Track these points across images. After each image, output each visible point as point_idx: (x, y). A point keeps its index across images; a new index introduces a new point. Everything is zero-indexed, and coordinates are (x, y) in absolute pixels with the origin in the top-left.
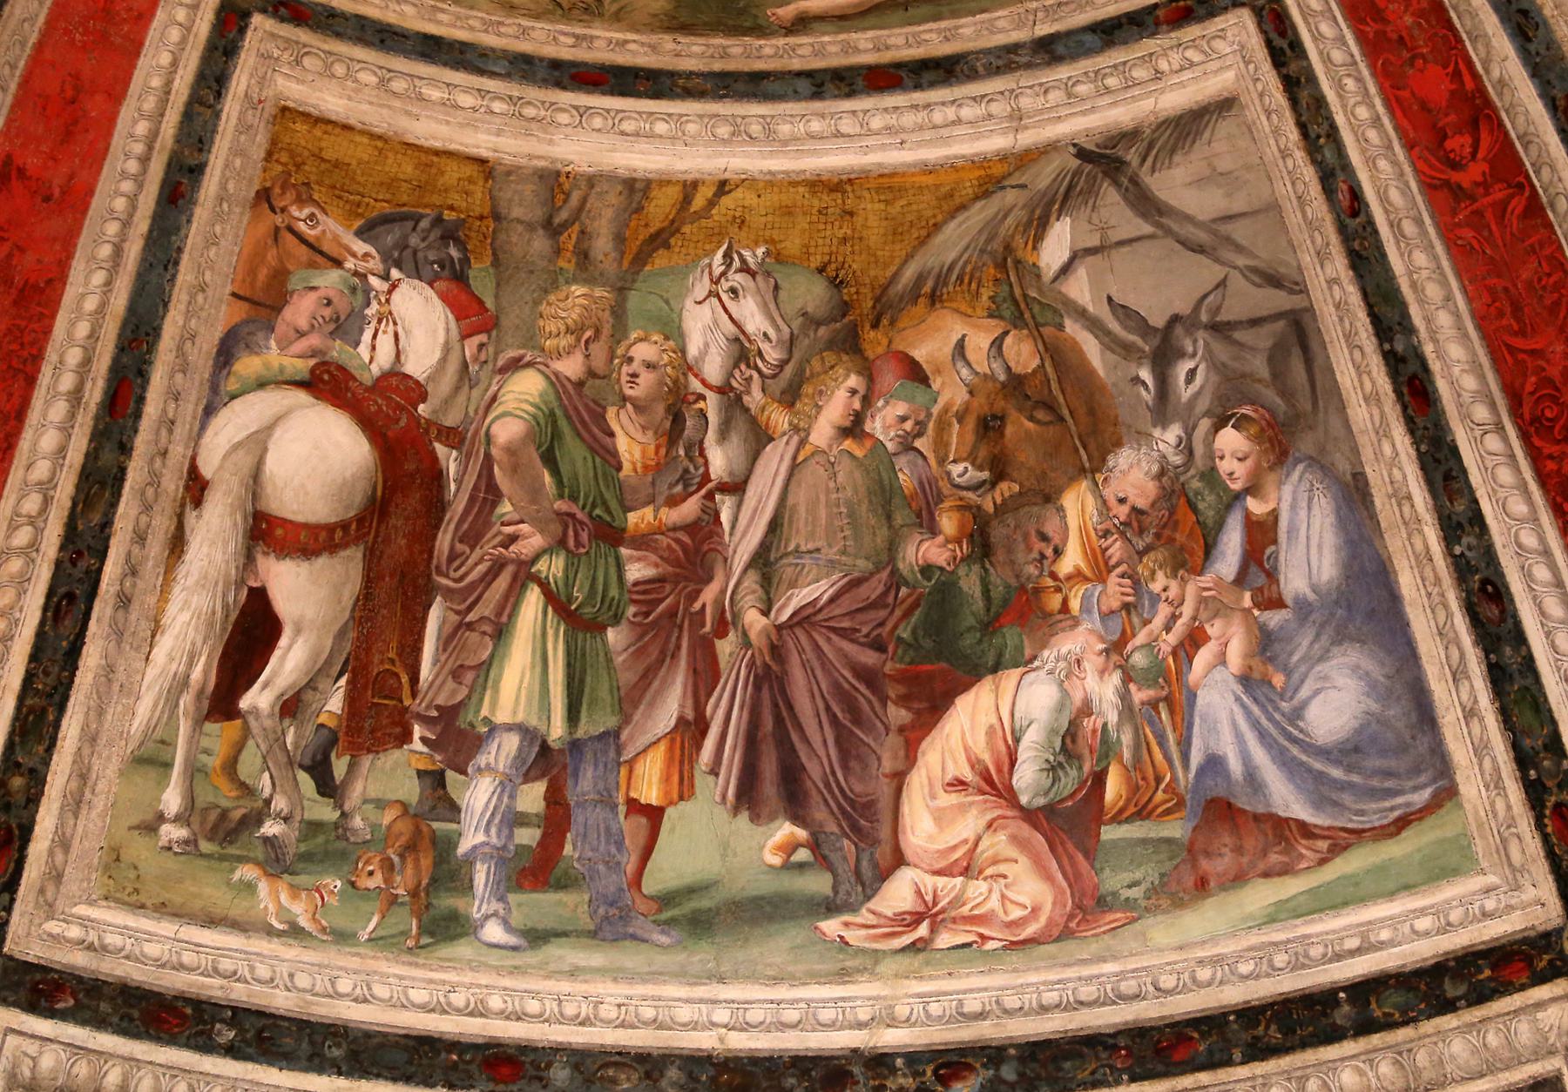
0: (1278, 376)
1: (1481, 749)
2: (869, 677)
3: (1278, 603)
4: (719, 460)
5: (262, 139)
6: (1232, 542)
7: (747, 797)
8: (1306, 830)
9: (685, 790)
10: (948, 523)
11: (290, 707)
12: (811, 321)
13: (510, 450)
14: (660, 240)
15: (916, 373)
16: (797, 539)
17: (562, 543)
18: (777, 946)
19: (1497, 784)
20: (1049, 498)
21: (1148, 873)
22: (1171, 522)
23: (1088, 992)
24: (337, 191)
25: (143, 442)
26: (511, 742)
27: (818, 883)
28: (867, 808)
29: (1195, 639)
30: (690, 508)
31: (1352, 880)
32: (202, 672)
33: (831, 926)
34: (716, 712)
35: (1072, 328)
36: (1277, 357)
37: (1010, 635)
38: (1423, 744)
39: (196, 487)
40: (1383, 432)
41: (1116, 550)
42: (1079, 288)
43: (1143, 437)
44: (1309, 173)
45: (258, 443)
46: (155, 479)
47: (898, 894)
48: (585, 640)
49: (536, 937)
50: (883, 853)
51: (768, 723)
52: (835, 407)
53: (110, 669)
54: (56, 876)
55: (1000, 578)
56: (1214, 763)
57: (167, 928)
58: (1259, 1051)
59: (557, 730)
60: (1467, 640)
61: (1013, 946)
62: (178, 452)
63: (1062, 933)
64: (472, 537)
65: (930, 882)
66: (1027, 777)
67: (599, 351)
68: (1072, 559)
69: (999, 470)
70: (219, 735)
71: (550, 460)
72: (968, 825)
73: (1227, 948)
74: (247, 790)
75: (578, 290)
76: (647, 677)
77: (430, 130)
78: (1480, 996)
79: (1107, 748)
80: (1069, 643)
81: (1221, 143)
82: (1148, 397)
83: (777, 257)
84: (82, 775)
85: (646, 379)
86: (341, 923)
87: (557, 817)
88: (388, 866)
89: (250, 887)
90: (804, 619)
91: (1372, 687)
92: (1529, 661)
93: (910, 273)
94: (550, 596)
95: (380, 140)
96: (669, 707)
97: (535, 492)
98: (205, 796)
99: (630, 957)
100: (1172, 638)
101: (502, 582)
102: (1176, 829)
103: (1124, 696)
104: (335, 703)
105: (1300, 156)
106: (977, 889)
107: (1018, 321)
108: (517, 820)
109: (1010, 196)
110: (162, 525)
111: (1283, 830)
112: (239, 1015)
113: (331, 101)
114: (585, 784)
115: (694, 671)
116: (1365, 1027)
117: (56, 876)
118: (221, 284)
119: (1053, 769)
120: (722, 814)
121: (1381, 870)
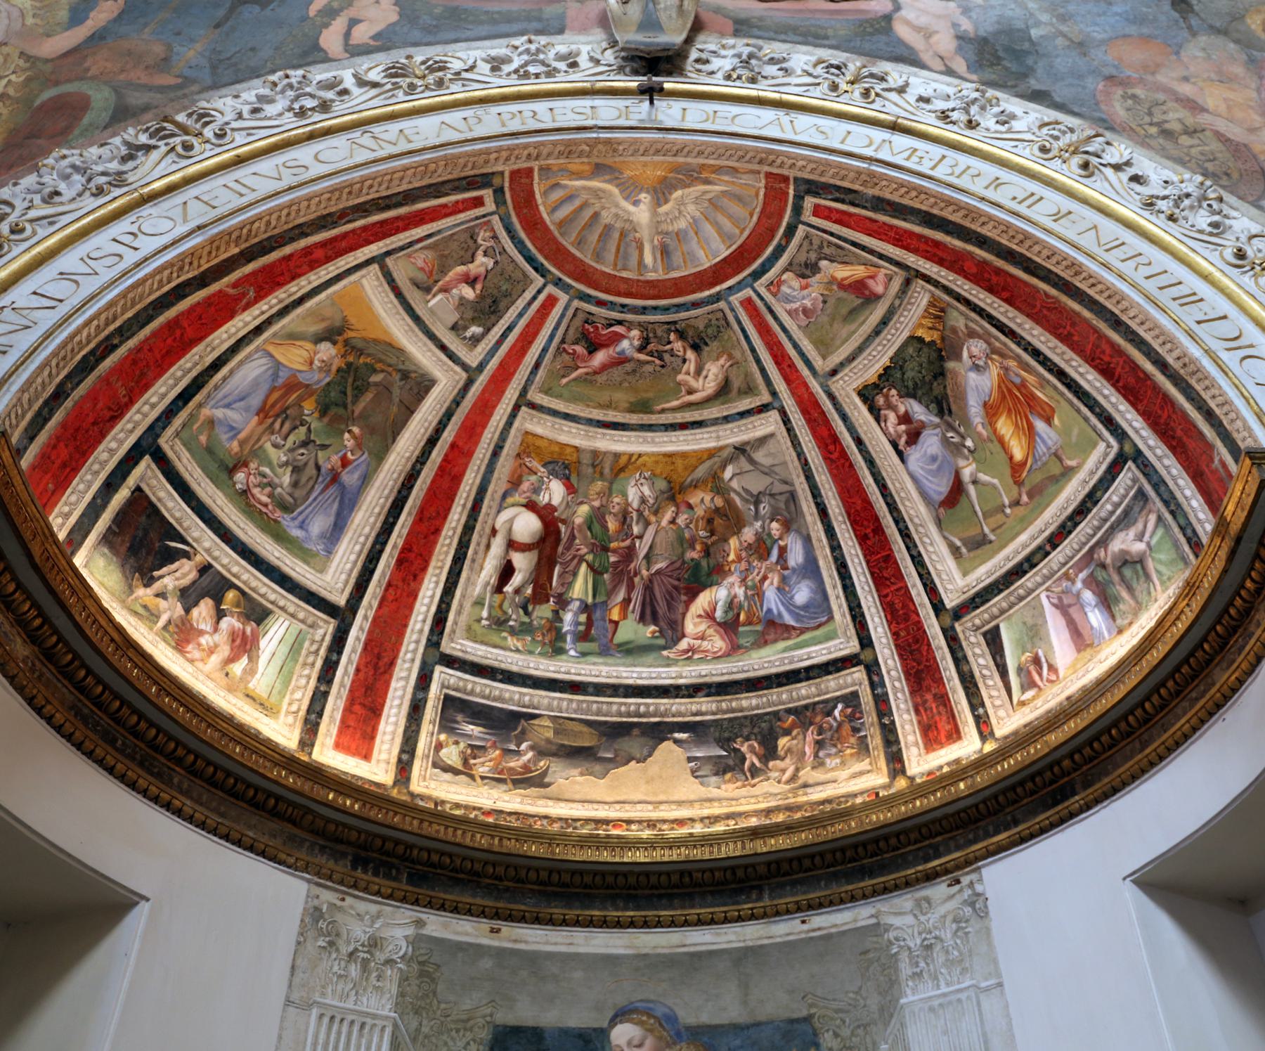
1: (840, 607)
2: (676, 588)
3: (787, 568)
4: (636, 530)
5: (520, 439)
8: (794, 628)
9: (625, 617)
10: (698, 547)
11: (517, 591)
12: (663, 492)
13: (579, 526)
14: (622, 470)
15: (690, 507)
17: (592, 551)
18: (650, 658)
19: (843, 615)
20: (726, 540)
21: (751, 639)
22: (759, 547)
23: (735, 670)
24: (538, 454)
25: (480, 519)
26: (577, 604)
27: (661, 642)
28: (675, 622)
29: (765, 578)
30: (628, 542)
31: (806, 641)
32: (493, 581)
33: (665, 653)
34: (634, 596)
35: (733, 495)
36: (787, 503)
37: (715, 578)
38: (825, 605)
39: (494, 532)
40: (815, 523)
41: (744, 554)
43: (751, 524)
44: (794, 454)
45: (511, 521)
46: (483, 529)
47: (683, 644)
48: (598, 577)
49: (584, 654)
50: (679, 634)
51: (648, 599)
52: (668, 515)
54: (453, 632)
55: (712, 562)
56: (769, 610)
57: (484, 648)
58: (780, 685)
59: (590, 600)
60: (837, 578)
61: (714, 658)
62: (490, 522)
63: (727, 655)
64: (568, 548)
65: (692, 642)
66: (719, 614)
67: (604, 499)
68: (732, 557)
69: (712, 533)
70: (498, 598)
71: (590, 529)
72: (703, 627)
73: (772, 658)
74: (505, 613)
76: (615, 588)
77: (563, 439)
78: (838, 670)
79: (741, 607)
80: (731, 579)
81: (771, 446)
82: (753, 513)
83: (654, 475)
84: (461, 605)
85: (617, 507)
86: (531, 649)
88: (543, 635)
89: (505, 638)
90: (658, 572)
91: (812, 590)
92: (853, 584)
93: (689, 480)
95: (551, 441)
96: (621, 595)
98: (494, 613)
99: (610, 660)
100: (758, 578)
101: (575, 561)
102: (759, 628)
103: (746, 593)
104: (529, 591)
105: (791, 449)
106: (705, 643)
107: (718, 493)
108: (578, 624)
109: (716, 459)
110: (484, 541)
111: (788, 628)
112: (503, 672)
113: (539, 430)
114: (597, 615)
115: (628, 586)
116: (808, 679)
117: (453, 632)
118: (505, 478)
119: (726, 612)
120: (635, 624)
121: (813, 638)
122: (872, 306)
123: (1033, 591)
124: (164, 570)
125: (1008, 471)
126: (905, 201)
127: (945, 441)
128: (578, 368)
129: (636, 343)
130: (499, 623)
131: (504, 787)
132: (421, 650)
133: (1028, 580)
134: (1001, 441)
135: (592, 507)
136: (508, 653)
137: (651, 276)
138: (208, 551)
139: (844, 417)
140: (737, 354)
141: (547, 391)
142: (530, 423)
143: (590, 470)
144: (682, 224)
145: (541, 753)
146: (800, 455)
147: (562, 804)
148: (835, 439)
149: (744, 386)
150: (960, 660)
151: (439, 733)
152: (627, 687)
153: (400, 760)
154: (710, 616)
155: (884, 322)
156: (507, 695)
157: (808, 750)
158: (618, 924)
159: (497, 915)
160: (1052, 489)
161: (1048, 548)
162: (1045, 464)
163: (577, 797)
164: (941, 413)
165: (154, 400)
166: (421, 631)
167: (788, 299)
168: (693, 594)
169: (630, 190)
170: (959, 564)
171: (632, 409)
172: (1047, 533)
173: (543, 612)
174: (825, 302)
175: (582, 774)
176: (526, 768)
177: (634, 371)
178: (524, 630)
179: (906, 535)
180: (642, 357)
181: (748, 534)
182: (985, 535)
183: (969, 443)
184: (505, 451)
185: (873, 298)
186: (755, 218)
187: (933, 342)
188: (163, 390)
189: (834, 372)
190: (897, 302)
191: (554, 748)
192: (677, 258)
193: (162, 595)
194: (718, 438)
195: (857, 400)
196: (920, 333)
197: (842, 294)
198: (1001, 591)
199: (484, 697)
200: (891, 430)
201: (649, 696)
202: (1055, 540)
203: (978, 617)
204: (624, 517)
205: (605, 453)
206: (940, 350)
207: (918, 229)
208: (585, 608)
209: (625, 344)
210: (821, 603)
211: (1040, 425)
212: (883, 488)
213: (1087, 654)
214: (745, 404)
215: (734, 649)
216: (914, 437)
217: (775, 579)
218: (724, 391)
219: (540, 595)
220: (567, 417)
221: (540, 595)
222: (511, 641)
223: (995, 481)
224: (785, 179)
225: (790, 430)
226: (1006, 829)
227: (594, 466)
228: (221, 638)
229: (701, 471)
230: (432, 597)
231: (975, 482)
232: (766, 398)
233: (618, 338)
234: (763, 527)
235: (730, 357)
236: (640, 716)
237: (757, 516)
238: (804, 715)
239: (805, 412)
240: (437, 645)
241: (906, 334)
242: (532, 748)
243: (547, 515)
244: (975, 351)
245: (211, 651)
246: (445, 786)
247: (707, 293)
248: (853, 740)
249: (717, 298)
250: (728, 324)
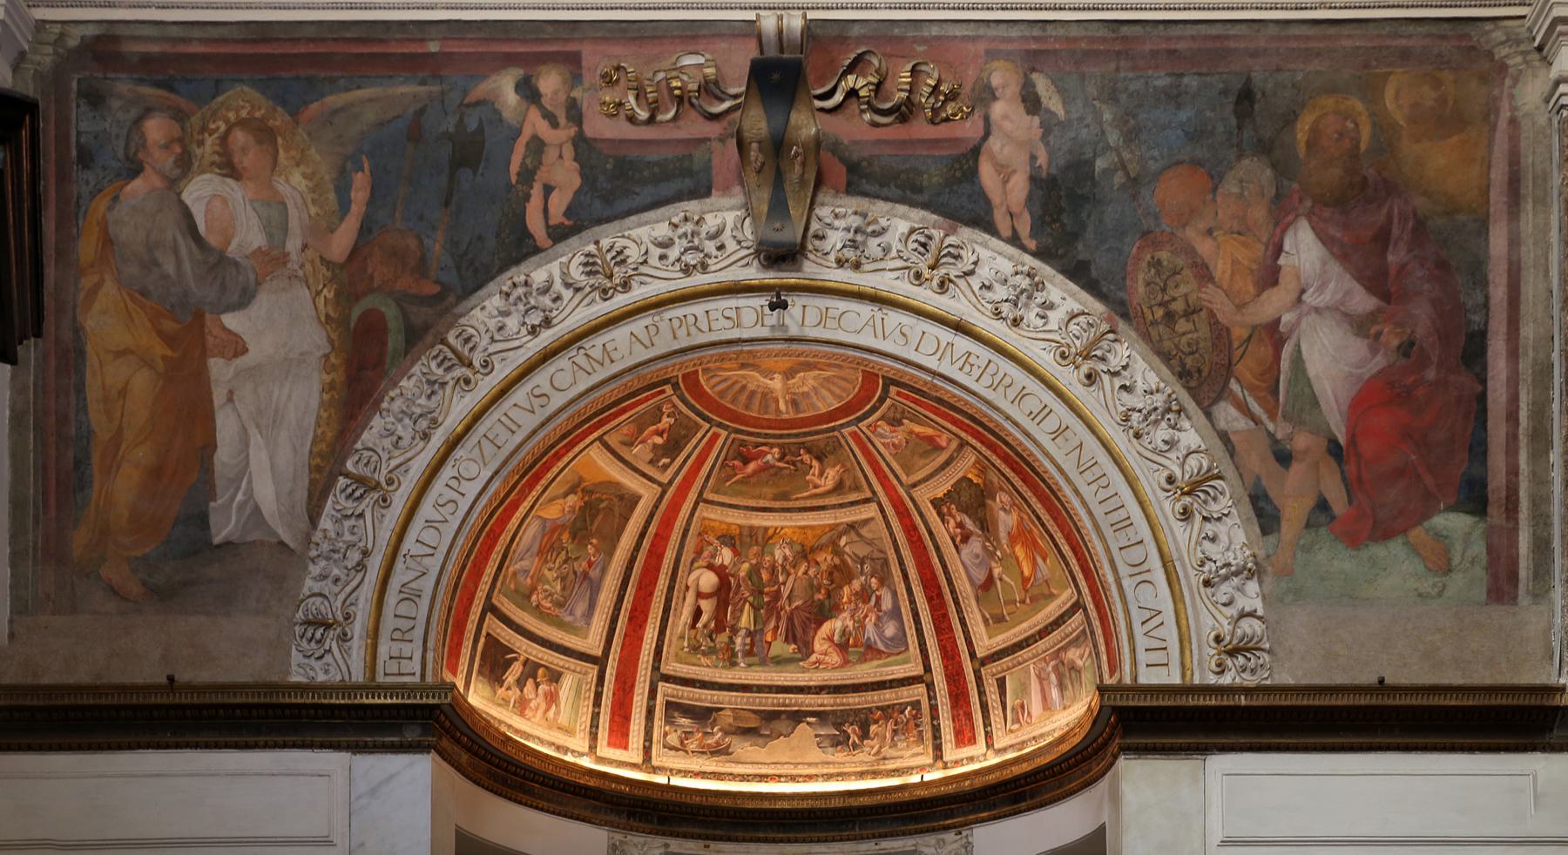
0: (882, 570)
2: (808, 619)
3: (881, 611)
4: (781, 579)
6: (873, 599)
7: (787, 640)
9: (775, 639)
10: (823, 591)
11: (705, 626)
12: (798, 553)
13: (743, 578)
15: (817, 563)
16: (795, 593)
18: (792, 667)
20: (842, 588)
21: (857, 657)
27: (799, 656)
29: (866, 616)
30: (776, 587)
33: (801, 663)
34: (781, 624)
35: (846, 556)
36: (882, 566)
37: (834, 613)
39: (687, 588)
41: (853, 598)
42: (847, 549)
44: (888, 534)
45: (698, 579)
47: (813, 658)
53: (673, 622)
54: (667, 658)
55: (832, 602)
56: (869, 639)
57: (687, 666)
59: (752, 628)
63: (841, 666)
64: (736, 594)
65: (819, 656)
66: (836, 638)
68: (845, 600)
69: (832, 582)
71: (750, 579)
72: (826, 646)
74: (698, 641)
75: (755, 548)
79: (850, 634)
80: (844, 615)
81: (872, 525)
84: (670, 641)
87: (752, 644)
89: (699, 659)
90: (796, 608)
94: (750, 604)
96: (772, 624)
97: (747, 585)
99: (766, 669)
102: (862, 650)
108: (745, 645)
110: (682, 595)
112: (700, 681)
117: (667, 658)
119: (841, 637)
122: (939, 453)
123: (1027, 661)
125: (1020, 581)
126: (957, 404)
127: (984, 547)
128: (736, 475)
129: (777, 456)
130: (695, 649)
131: (705, 757)
132: (649, 674)
133: (1024, 653)
134: (1017, 559)
135: (751, 564)
136: (702, 669)
137: (785, 416)
139: (921, 515)
140: (849, 465)
141: (716, 491)
142: (705, 512)
143: (748, 539)
144: (805, 389)
145: (726, 733)
146: (892, 534)
147: (740, 766)
148: (915, 528)
149: (853, 486)
150: (982, 693)
151: (665, 726)
152: (778, 687)
153: (644, 747)
154: (830, 639)
155: (947, 463)
156: (703, 697)
157: (888, 735)
158: (774, 841)
159: (707, 838)
160: (1042, 602)
161: (1037, 637)
162: (1041, 584)
163: (749, 760)
164: (982, 528)
166: (648, 661)
167: (881, 436)
168: (819, 624)
169: (768, 374)
170: (987, 630)
171: (776, 498)
172: (1038, 628)
173: (722, 638)
174: (907, 443)
175: (751, 746)
176: (718, 744)
177: (776, 474)
178: (712, 651)
179: (957, 603)
180: (781, 464)
181: (856, 585)
182: (1004, 616)
183: (998, 553)
184: (690, 532)
185: (939, 449)
186: (856, 390)
187: (977, 485)
189: (914, 485)
190: (955, 454)
191: (733, 729)
192: (803, 406)
194: (836, 518)
195: (930, 505)
196: (970, 476)
197: (918, 440)
198: (1009, 655)
199: (689, 700)
200: (951, 530)
201: (792, 693)
202: (1044, 633)
203: (994, 667)
204: (773, 570)
205: (758, 528)
206: (982, 491)
207: (967, 421)
208: (750, 634)
209: (769, 457)
210: (900, 639)
211: (1039, 560)
212: (945, 567)
213: (1048, 713)
214: (854, 497)
215: (846, 663)
216: (966, 538)
217: (872, 617)
218: (839, 488)
219: (720, 628)
220: (731, 506)
221: (720, 628)
222: (704, 660)
223: (1012, 583)
224: (877, 375)
225: (885, 517)
226: (990, 810)
227: (751, 537)
229: (824, 540)
230: (652, 638)
231: (1001, 579)
232: (869, 494)
233: (765, 454)
234: (866, 580)
235: (843, 466)
236: (786, 706)
237: (862, 573)
238: (887, 711)
239: (894, 506)
240: (658, 669)
241: (961, 475)
242: (721, 730)
243: (720, 571)
244: (1004, 500)
246: (671, 759)
247: (825, 426)
248: (915, 732)
249: (833, 429)
250: (841, 446)
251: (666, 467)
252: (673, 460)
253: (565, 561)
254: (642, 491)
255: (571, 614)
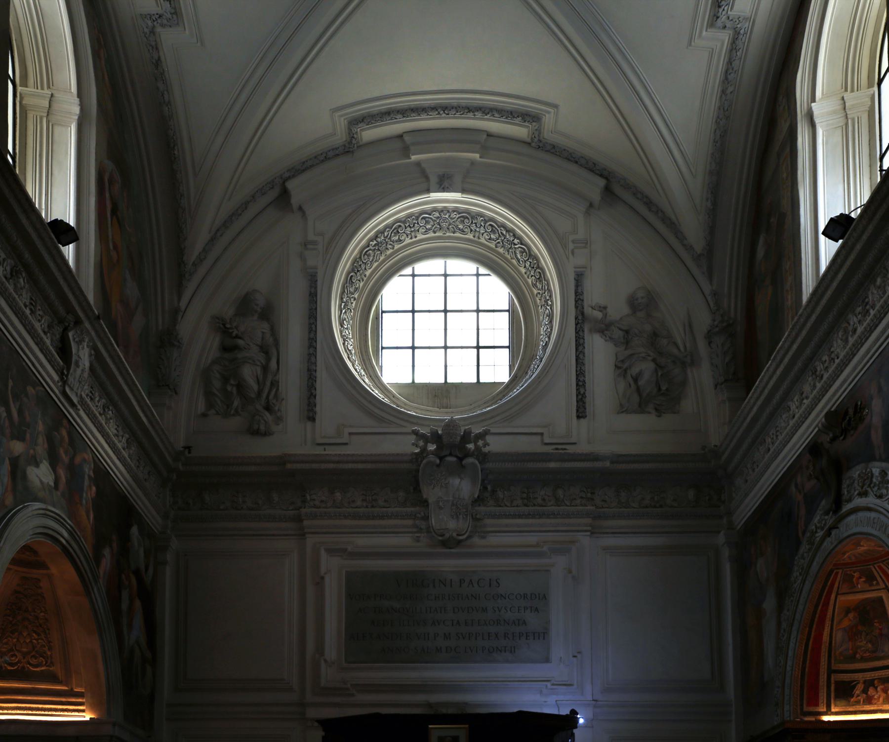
124: (855, 691)
138: (862, 678)
165: (823, 664)
188: (823, 660)
193: (858, 696)
228: (880, 693)
245: (879, 697)
251: (878, 584)
252: (877, 580)
253: (867, 634)
254: (880, 595)
255: (883, 652)
